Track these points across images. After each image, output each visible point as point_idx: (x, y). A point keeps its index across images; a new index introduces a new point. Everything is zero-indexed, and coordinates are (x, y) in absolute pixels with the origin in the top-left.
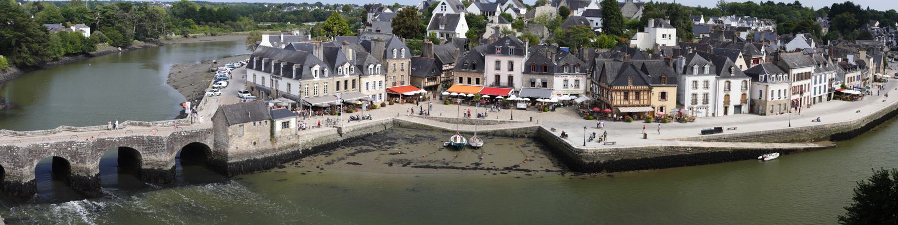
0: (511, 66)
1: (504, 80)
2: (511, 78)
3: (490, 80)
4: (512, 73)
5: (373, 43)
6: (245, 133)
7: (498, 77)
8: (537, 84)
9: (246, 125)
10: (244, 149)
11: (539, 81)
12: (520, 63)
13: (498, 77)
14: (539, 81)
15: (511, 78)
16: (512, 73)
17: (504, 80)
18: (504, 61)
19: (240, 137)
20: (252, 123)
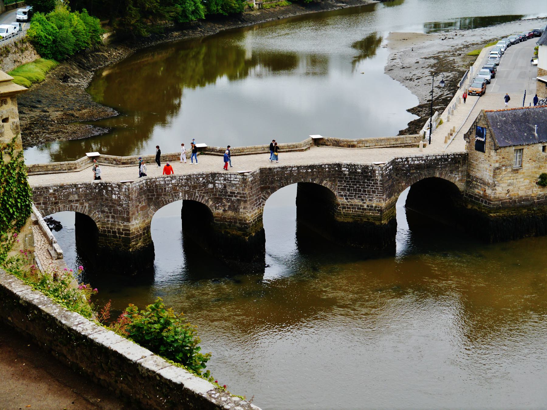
6: (527, 165)
9: (528, 151)
10: (521, 193)
19: (516, 171)
20: (540, 147)
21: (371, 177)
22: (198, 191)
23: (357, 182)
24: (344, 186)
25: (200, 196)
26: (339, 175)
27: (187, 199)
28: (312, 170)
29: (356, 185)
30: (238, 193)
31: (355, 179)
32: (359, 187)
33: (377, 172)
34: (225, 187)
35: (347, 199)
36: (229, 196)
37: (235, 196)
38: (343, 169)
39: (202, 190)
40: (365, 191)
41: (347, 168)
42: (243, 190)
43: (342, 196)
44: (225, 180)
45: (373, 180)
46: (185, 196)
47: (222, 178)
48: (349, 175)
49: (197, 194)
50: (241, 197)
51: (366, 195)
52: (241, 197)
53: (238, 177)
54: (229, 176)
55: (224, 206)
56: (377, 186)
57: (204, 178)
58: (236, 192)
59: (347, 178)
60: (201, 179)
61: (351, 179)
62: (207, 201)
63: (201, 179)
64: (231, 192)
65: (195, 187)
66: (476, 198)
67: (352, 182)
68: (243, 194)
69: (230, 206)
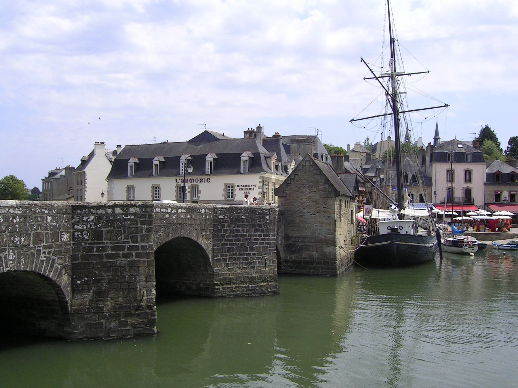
0: (468, 176)
1: (459, 194)
2: (468, 192)
3: (441, 195)
4: (469, 185)
5: (294, 146)
7: (451, 192)
8: (503, 198)
11: (505, 195)
12: (480, 172)
13: (451, 192)
14: (505, 195)
15: (468, 192)
16: (469, 185)
17: (459, 194)
18: (459, 169)
21: (260, 225)
22: (45, 247)
23: (242, 236)
24: (223, 245)
25: (48, 259)
26: (214, 226)
27: (22, 268)
28: (191, 215)
29: (239, 240)
30: (131, 248)
31: (238, 231)
32: (244, 244)
33: (268, 217)
34: (98, 235)
35: (227, 265)
36: (109, 256)
37: (125, 256)
38: (221, 217)
39: (51, 247)
40: (252, 249)
41: (225, 214)
42: (143, 241)
43: (219, 260)
44: (99, 218)
45: (262, 231)
46: (19, 259)
47: (92, 218)
48: (229, 226)
49: (42, 257)
50: (137, 255)
51: (254, 254)
52: (138, 255)
53: (132, 210)
54: (110, 211)
55: (99, 281)
56: (268, 240)
57: (54, 217)
58: (127, 245)
59: (225, 231)
60: (49, 219)
61: (231, 231)
62: (60, 275)
63: (49, 219)
64: (113, 248)
65: (38, 239)
66: (306, 262)
67: (233, 236)
68: (144, 247)
69: (110, 282)
